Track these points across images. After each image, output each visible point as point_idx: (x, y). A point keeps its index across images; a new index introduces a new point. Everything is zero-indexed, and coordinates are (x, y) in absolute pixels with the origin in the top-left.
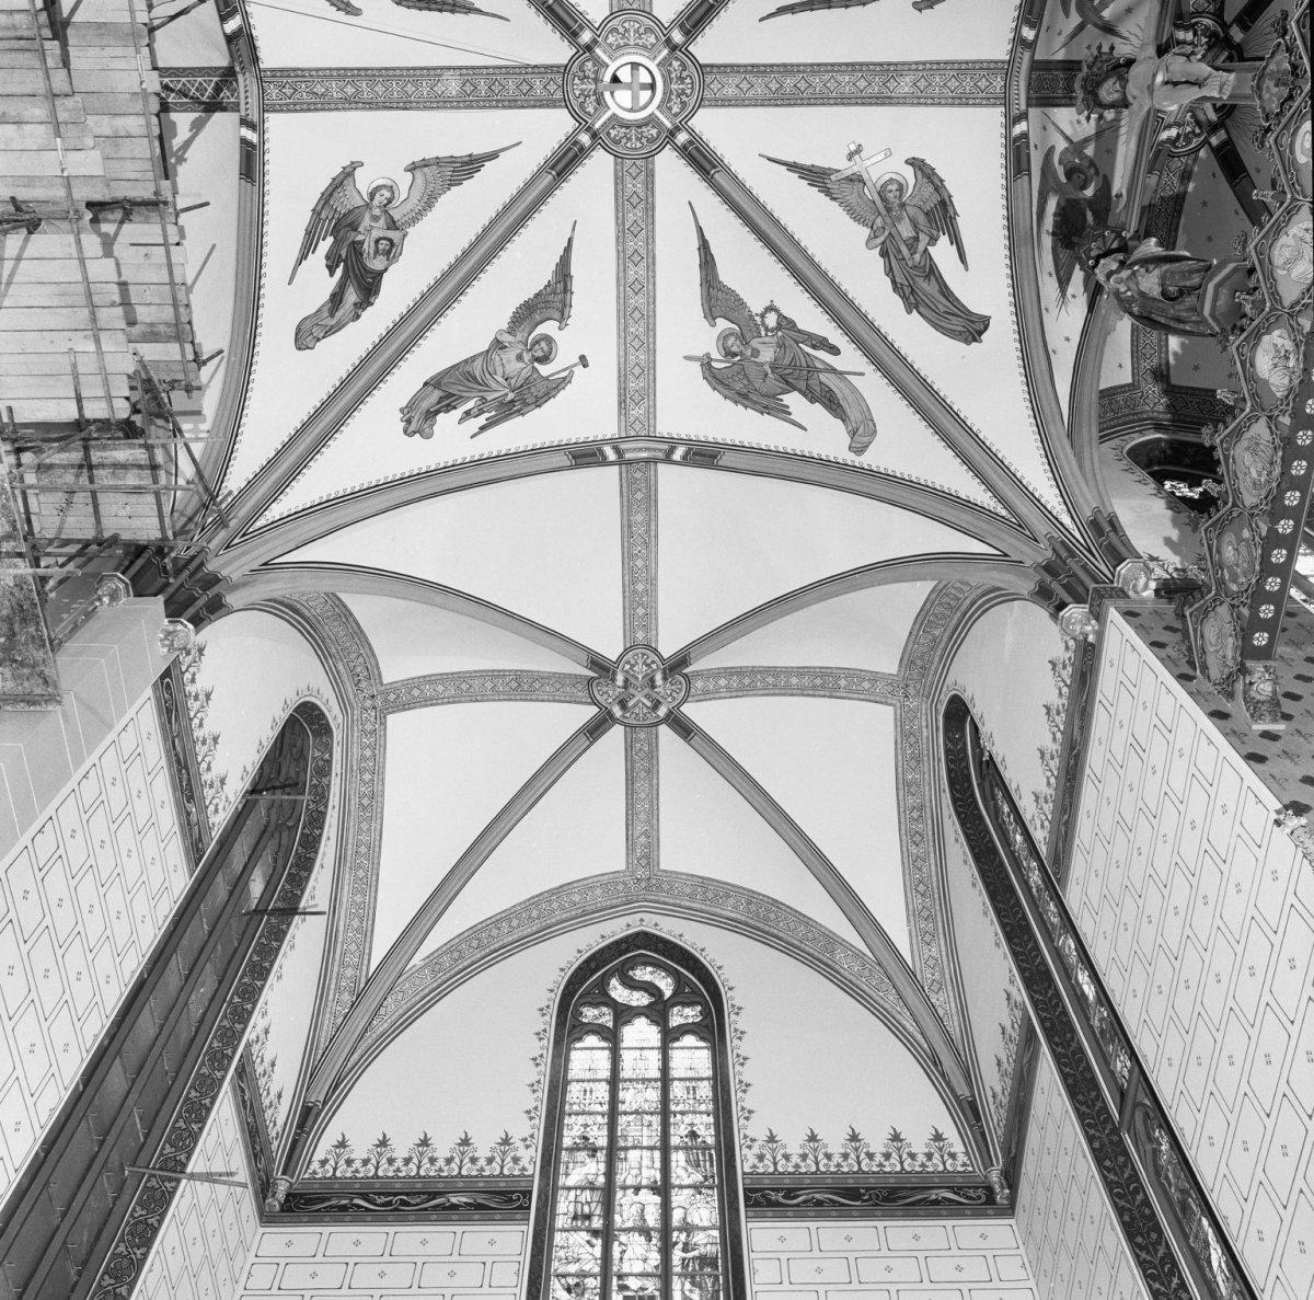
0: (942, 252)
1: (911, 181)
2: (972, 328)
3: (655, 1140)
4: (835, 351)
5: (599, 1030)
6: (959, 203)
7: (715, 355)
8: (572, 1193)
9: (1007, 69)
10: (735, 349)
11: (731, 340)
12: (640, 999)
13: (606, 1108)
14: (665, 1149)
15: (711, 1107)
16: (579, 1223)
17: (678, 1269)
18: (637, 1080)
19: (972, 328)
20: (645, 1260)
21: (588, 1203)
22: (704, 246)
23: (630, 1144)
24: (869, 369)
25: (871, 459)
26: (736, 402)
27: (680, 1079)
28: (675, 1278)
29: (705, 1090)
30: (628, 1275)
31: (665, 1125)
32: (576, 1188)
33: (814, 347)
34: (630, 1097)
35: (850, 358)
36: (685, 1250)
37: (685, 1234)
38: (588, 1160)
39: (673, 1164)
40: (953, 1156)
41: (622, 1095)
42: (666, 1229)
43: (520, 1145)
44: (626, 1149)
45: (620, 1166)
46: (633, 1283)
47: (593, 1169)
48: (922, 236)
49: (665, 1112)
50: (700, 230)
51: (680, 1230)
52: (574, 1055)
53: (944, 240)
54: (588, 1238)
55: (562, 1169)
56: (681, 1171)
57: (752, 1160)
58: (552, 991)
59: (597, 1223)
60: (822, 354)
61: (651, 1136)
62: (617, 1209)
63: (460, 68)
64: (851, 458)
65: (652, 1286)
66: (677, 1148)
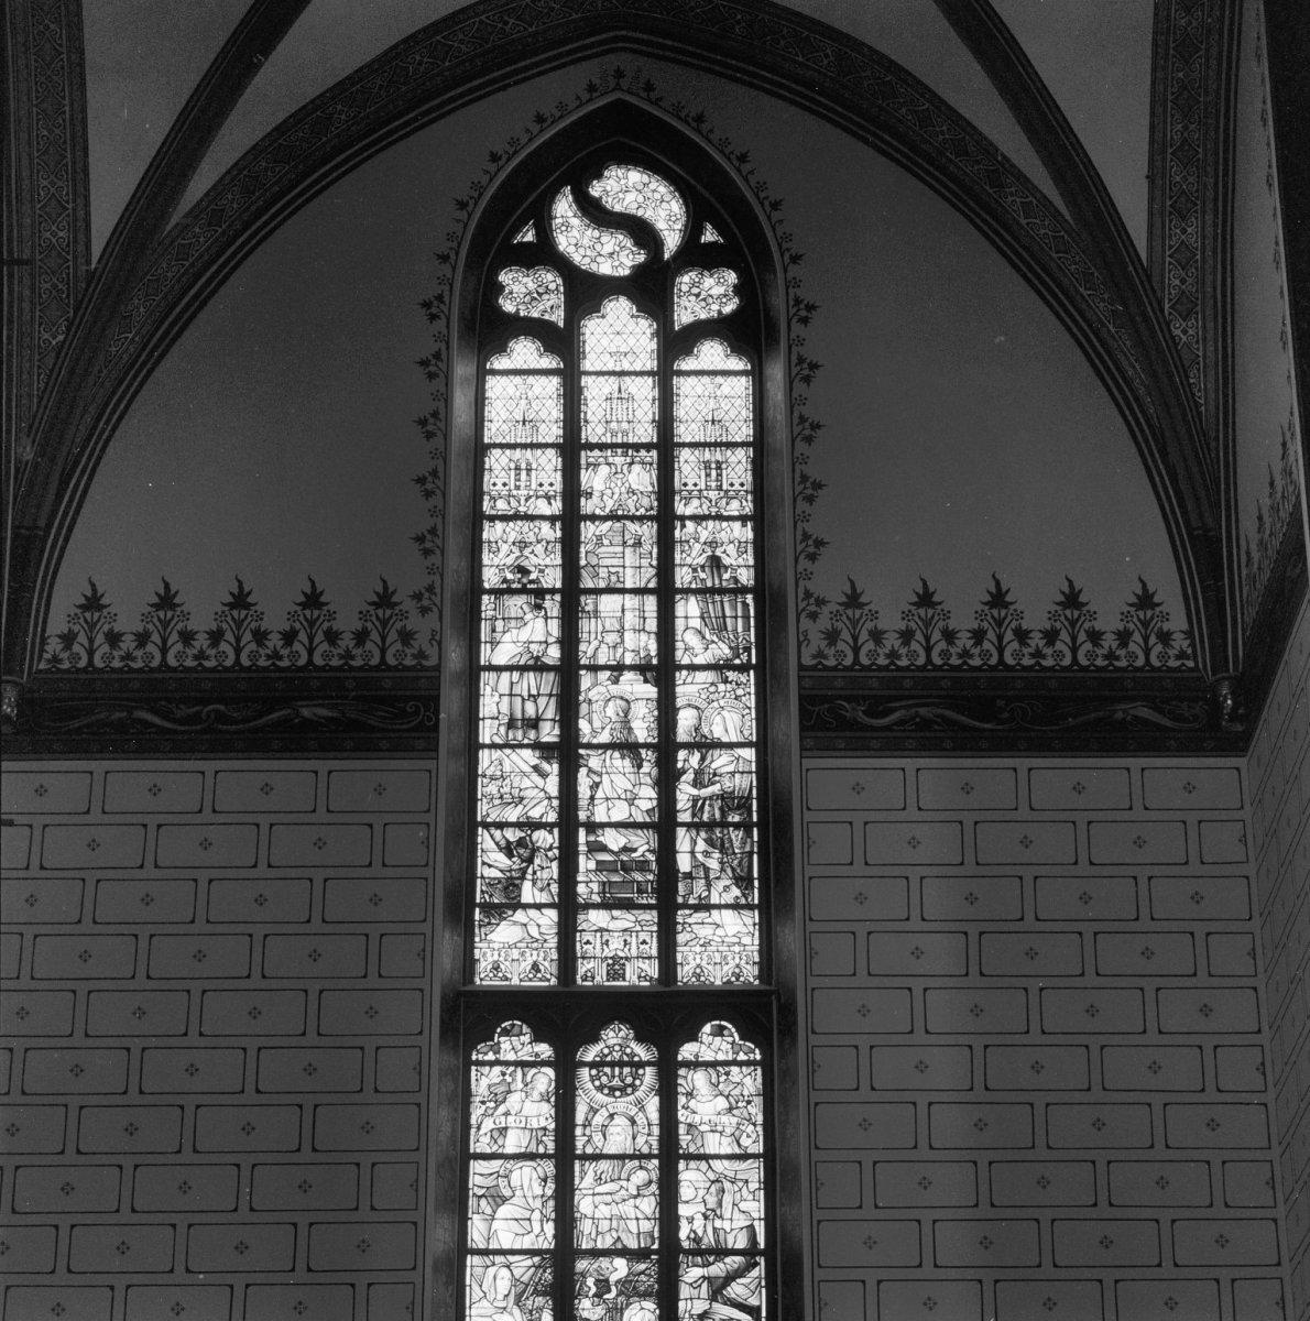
3: (648, 577)
5: (540, 330)
8: (505, 676)
12: (613, 256)
13: (557, 507)
14: (665, 592)
15: (749, 508)
16: (519, 735)
17: (685, 817)
18: (613, 446)
20: (631, 802)
21: (534, 698)
23: (602, 585)
27: (694, 445)
28: (681, 832)
29: (739, 468)
30: (603, 825)
31: (666, 544)
32: (510, 668)
34: (602, 483)
36: (697, 783)
37: (697, 756)
38: (529, 616)
39: (680, 624)
40: (1165, 638)
41: (586, 478)
42: (666, 746)
43: (409, 605)
44: (597, 592)
45: (586, 626)
46: (614, 840)
47: (534, 632)
49: (665, 519)
51: (688, 746)
52: (494, 386)
54: (536, 761)
55: (485, 627)
56: (693, 644)
57: (817, 641)
58: (444, 258)
59: (549, 733)
61: (638, 569)
62: (584, 708)
65: (643, 844)
66: (687, 591)
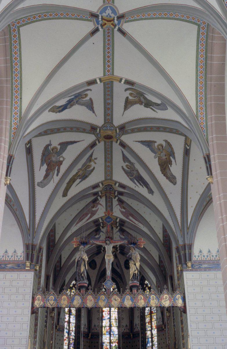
0: (78, 180)
1: (90, 169)
2: (65, 195)
4: (57, 175)
6: (87, 179)
7: (52, 147)
9: (111, 179)
10: (54, 151)
11: (56, 150)
19: (65, 195)
22: (75, 142)
24: (55, 184)
25: (37, 189)
26: (42, 153)
33: (57, 170)
35: (56, 179)
48: (80, 177)
50: (79, 141)
53: (80, 180)
60: (56, 172)
63: (113, 103)
64: (36, 183)
